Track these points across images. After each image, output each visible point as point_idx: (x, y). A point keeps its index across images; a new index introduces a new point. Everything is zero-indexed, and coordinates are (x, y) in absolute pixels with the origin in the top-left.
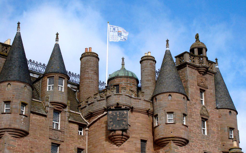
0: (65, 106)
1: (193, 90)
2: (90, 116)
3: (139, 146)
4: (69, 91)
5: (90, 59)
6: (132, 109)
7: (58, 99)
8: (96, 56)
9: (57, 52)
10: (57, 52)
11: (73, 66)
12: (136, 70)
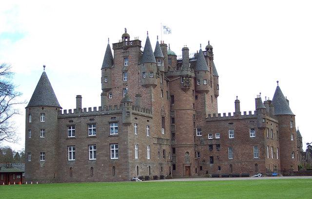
2: (172, 77)
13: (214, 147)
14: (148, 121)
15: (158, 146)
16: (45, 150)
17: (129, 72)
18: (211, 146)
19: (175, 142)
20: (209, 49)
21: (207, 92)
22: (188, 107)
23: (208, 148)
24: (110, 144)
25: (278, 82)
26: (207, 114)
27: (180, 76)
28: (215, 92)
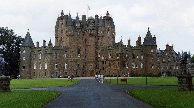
1: (106, 25)
5: (84, 16)
6: (93, 30)
7: (78, 28)
9: (77, 16)
10: (77, 16)
11: (81, 18)
12: (94, 18)
13: (104, 62)
16: (25, 65)
18: (103, 62)
19: (86, 60)
20: (108, 14)
22: (92, 44)
23: (102, 62)
25: (149, 28)
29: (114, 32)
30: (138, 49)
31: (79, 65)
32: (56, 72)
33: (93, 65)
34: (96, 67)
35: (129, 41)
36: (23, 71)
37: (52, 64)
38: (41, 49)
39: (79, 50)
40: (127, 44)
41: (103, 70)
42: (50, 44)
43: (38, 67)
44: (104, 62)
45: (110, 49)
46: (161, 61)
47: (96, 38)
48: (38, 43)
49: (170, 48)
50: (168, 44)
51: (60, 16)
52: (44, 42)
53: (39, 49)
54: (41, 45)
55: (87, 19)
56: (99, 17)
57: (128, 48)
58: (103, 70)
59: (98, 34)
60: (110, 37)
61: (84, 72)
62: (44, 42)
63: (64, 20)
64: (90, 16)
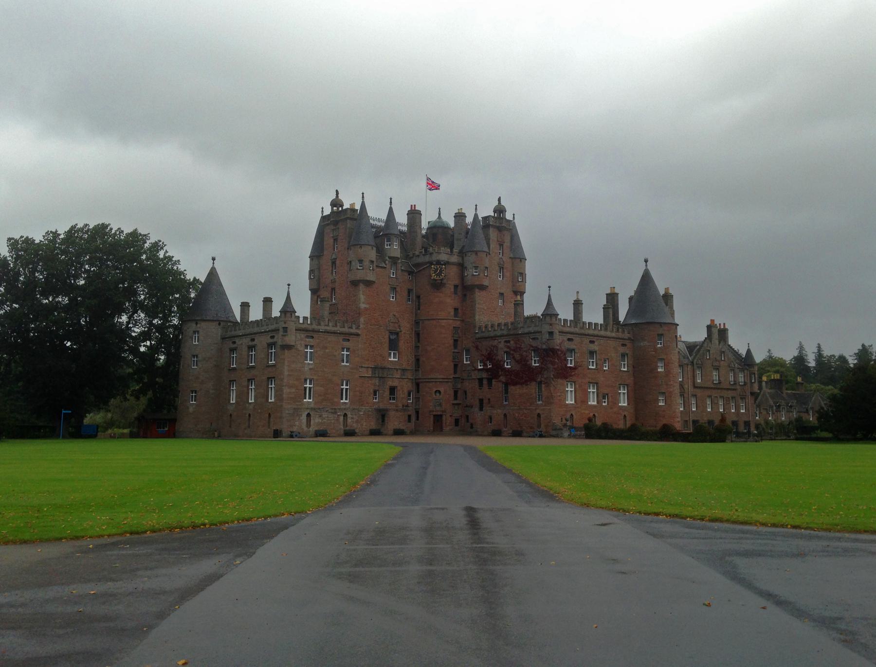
0: (398, 258)
1: (493, 245)
2: (417, 265)
3: (453, 290)
4: (402, 245)
5: (414, 215)
6: (447, 263)
7: (392, 255)
8: (419, 213)
11: (402, 218)
13: (485, 382)
14: (344, 340)
15: (377, 381)
17: (338, 262)
18: (481, 380)
20: (500, 210)
21: (482, 288)
24: (268, 378)
26: (478, 325)
27: (429, 262)
28: (513, 286)
29: (523, 274)
30: (608, 334)
31: (392, 390)
32: (309, 415)
33: (447, 390)
34: (456, 398)
35: (577, 304)
36: (191, 410)
37: (290, 387)
38: (256, 330)
39: (393, 337)
40: (570, 317)
41: (481, 409)
42: (288, 310)
43: (243, 396)
44: (485, 382)
45: (505, 332)
46: (690, 383)
47: (455, 293)
48: (245, 306)
49: (718, 333)
50: (712, 321)
51: (328, 211)
52: (267, 301)
53: (248, 331)
54: (256, 314)
55: (424, 225)
56: (469, 220)
57: (572, 330)
58: (481, 409)
59: (462, 277)
60: (508, 293)
61: (409, 416)
62: (267, 301)
63: (342, 227)
64: (434, 218)
